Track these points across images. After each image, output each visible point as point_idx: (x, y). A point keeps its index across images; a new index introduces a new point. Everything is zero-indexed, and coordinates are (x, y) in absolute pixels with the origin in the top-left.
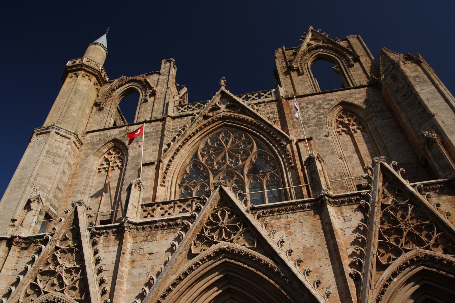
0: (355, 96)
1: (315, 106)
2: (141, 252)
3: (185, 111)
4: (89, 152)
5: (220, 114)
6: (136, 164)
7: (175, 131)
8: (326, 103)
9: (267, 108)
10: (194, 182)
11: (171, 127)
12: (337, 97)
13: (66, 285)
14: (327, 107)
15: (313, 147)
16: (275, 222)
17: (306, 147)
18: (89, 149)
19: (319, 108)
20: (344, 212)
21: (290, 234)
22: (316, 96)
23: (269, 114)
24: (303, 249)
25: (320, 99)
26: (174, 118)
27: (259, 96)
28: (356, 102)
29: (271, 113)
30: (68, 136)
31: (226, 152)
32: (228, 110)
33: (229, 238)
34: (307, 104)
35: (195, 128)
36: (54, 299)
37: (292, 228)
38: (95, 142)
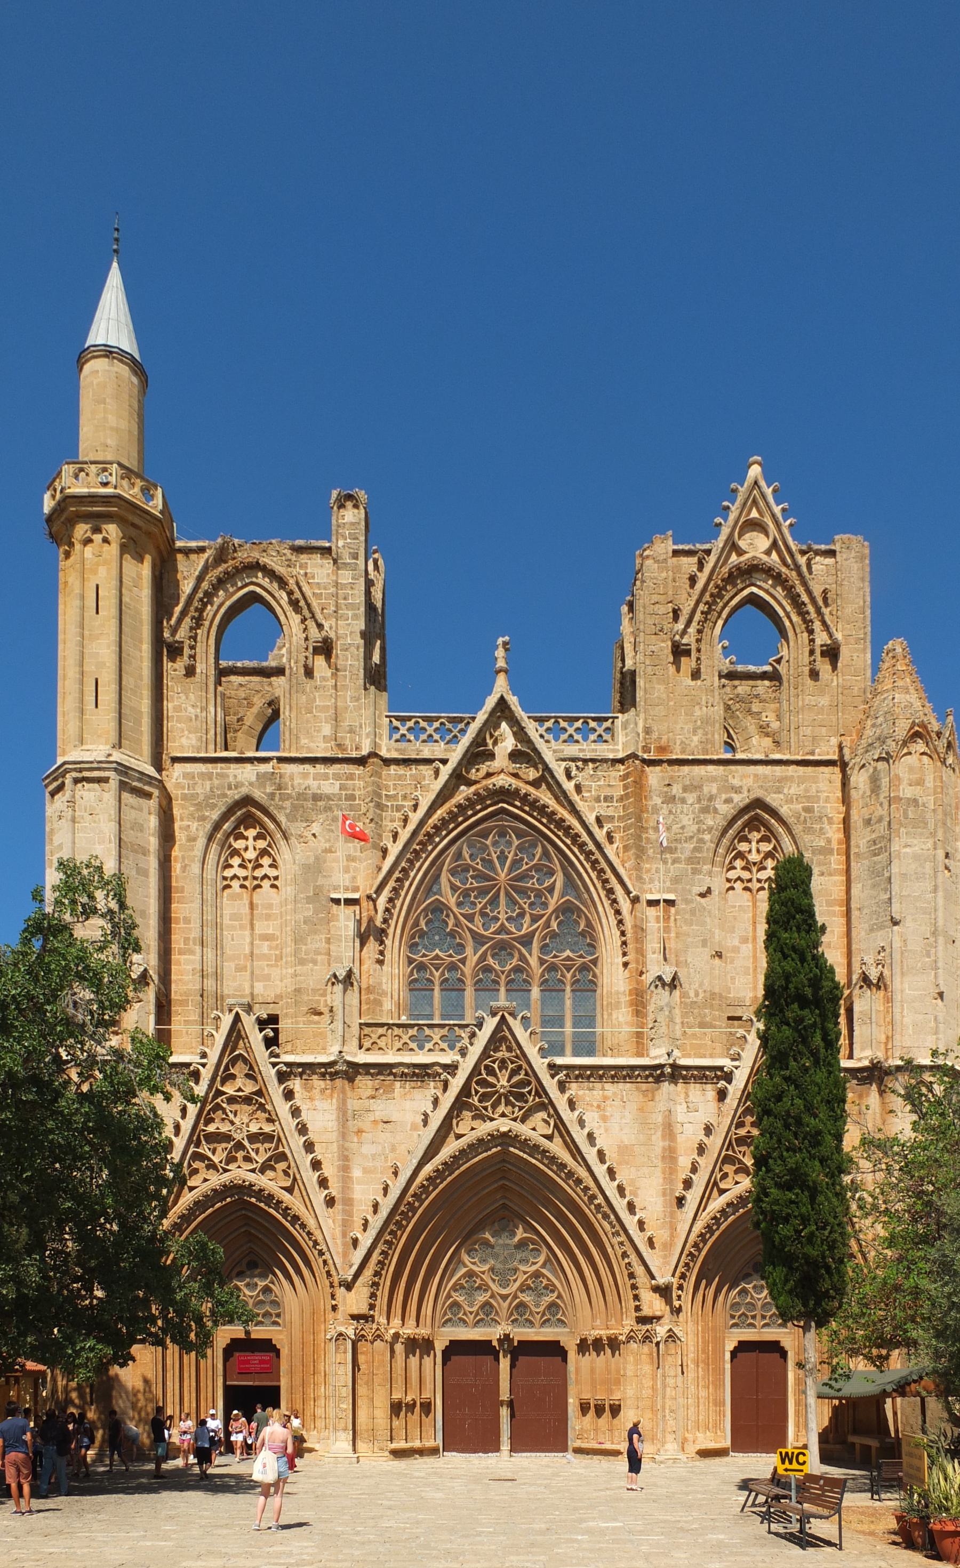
0: (790, 788)
1: (699, 800)
3: (409, 741)
4: (194, 825)
5: (493, 780)
6: (314, 890)
7: (392, 805)
8: (724, 796)
9: (599, 780)
11: (384, 793)
12: (750, 782)
13: (257, 1162)
15: (672, 924)
16: (584, 1094)
17: (658, 919)
18: (192, 816)
19: (705, 810)
20: (690, 1094)
21: (604, 1119)
22: (711, 768)
23: (600, 801)
24: (619, 1147)
25: (713, 779)
27: (585, 731)
28: (784, 811)
29: (606, 799)
31: (500, 888)
32: (512, 767)
33: (513, 1113)
34: (685, 789)
35: (439, 812)
36: (244, 1182)
37: (609, 1109)
38: (201, 797)
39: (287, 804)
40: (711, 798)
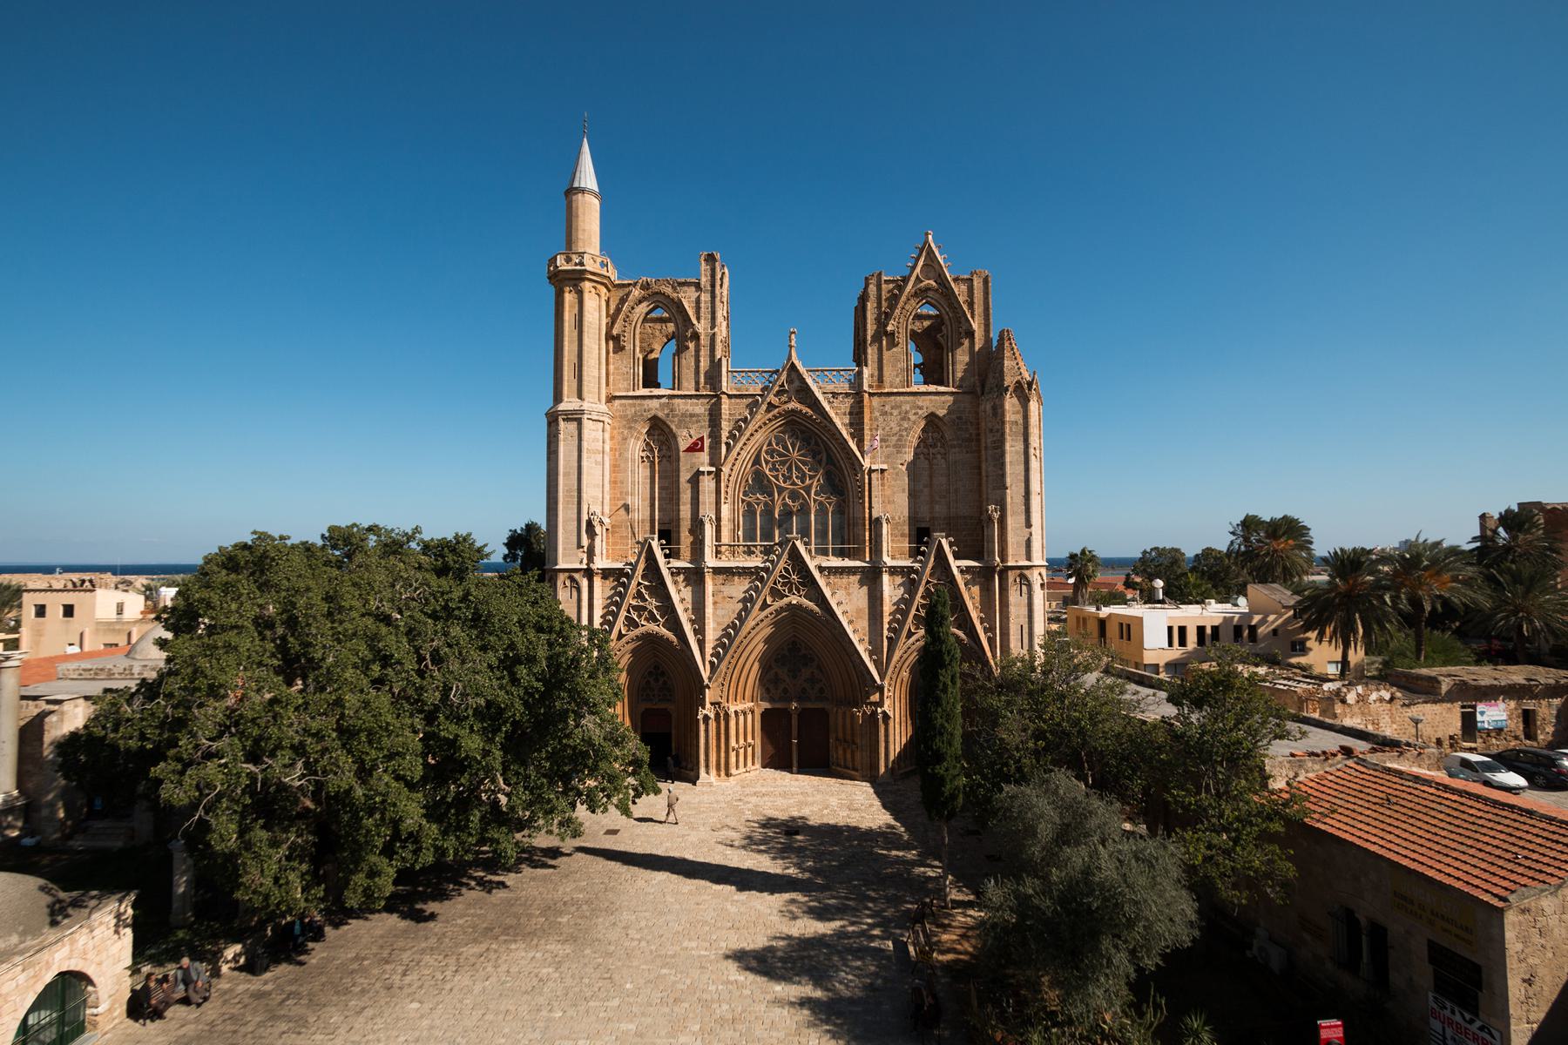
1: (900, 413)
2: (721, 595)
10: (758, 499)
14: (913, 418)
18: (625, 426)
19: (903, 419)
21: (849, 594)
25: (908, 402)
26: (730, 396)
28: (945, 420)
30: (601, 419)
39: (676, 419)
40: (907, 412)
